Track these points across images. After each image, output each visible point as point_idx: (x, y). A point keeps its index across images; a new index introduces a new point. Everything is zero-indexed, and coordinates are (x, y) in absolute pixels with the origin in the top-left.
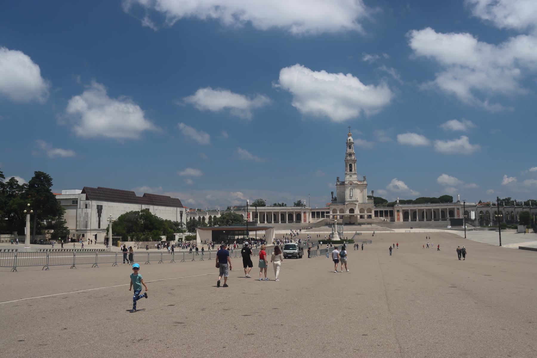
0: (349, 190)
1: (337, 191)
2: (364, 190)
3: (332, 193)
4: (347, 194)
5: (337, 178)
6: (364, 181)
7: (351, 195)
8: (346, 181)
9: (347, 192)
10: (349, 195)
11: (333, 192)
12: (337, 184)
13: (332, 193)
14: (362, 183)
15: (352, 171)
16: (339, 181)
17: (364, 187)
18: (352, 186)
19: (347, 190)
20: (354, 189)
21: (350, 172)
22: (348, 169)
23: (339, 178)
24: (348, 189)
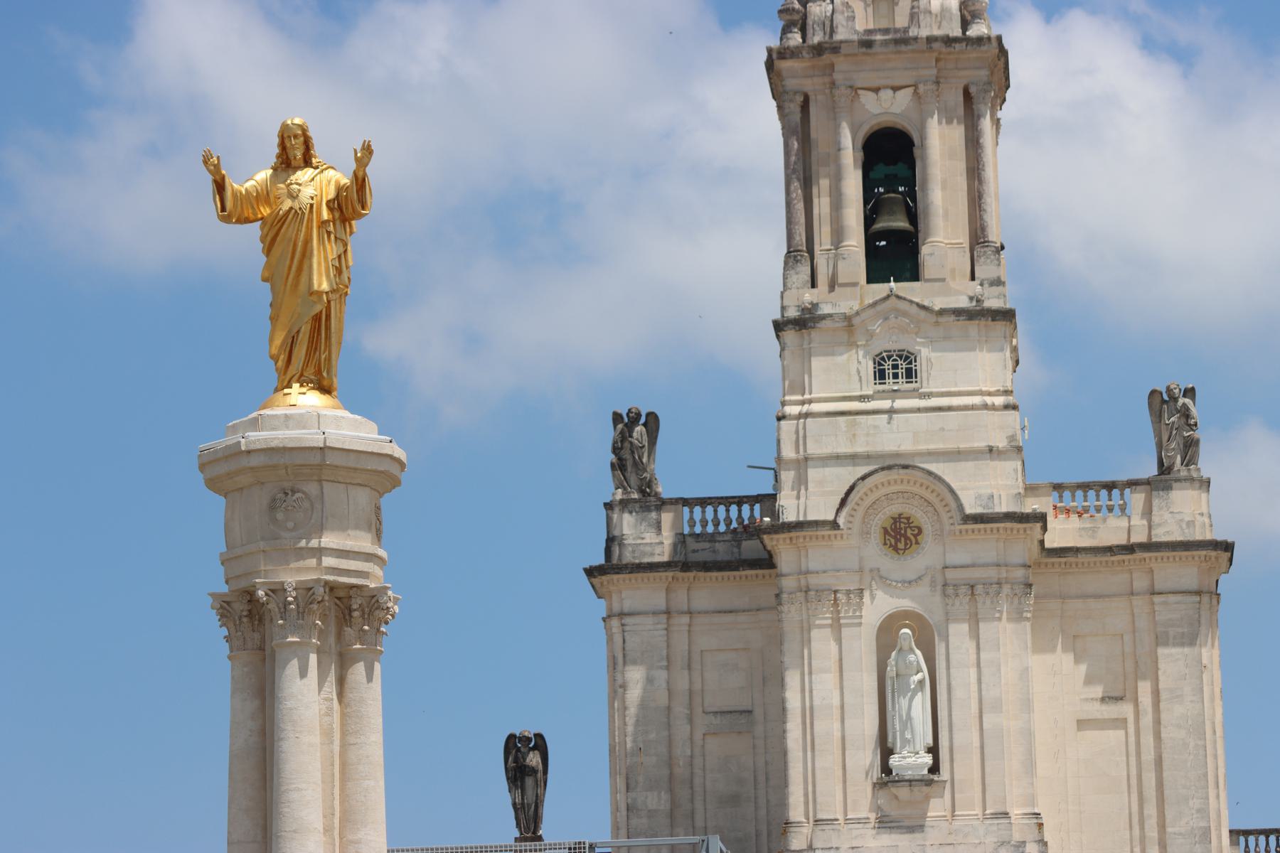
0: (862, 644)
1: (617, 689)
2: (1172, 660)
4: (827, 727)
5: (625, 422)
6: (1164, 478)
7: (911, 760)
8: (803, 463)
9: (825, 687)
10: (865, 757)
11: (540, 744)
12: (612, 541)
14: (1112, 531)
15: (913, 273)
16: (646, 488)
17: (1172, 610)
18: (927, 556)
19: (822, 644)
20: (959, 632)
21: (880, 289)
22: (838, 235)
23: (652, 422)
24: (837, 627)
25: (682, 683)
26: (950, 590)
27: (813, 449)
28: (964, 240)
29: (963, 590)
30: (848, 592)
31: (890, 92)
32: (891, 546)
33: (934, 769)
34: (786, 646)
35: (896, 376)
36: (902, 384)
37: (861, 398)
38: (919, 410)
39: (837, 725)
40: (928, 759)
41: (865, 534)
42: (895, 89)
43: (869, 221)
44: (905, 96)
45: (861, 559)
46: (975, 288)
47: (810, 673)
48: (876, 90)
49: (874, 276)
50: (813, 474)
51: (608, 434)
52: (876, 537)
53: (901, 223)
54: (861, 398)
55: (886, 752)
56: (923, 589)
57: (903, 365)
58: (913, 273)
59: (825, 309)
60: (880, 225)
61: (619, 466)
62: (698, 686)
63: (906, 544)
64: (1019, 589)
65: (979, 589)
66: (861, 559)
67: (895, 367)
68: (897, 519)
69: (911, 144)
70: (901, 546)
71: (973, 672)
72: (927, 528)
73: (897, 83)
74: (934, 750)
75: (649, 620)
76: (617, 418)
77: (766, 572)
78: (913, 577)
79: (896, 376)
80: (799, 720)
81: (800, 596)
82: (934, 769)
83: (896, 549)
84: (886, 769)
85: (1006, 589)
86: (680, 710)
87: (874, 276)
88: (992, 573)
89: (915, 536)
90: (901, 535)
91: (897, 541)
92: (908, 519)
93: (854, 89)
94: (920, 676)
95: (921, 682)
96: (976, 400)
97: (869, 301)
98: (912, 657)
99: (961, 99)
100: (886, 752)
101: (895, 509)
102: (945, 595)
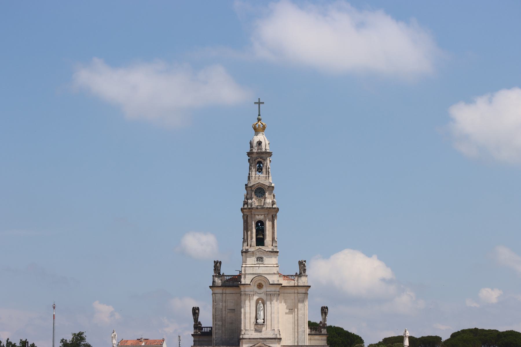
0: (253, 303)
2: (300, 305)
3: (195, 312)
4: (248, 315)
6: (299, 275)
8: (245, 274)
9: (248, 309)
11: (198, 309)
12: (214, 282)
13: (195, 312)
14: (292, 283)
15: (263, 245)
16: (219, 273)
17: (301, 296)
18: (264, 290)
19: (247, 302)
20: (268, 303)
21: (258, 247)
22: (252, 238)
23: (220, 263)
24: (250, 300)
25: (224, 305)
26: (267, 295)
27: (247, 272)
28: (271, 239)
29: (269, 295)
30: (252, 295)
34: (242, 303)
36: (261, 262)
37: (255, 264)
38: (263, 267)
39: (249, 315)
41: (254, 286)
42: (261, 215)
43: (257, 235)
44: (263, 216)
46: (272, 247)
47: (245, 307)
48: (258, 215)
49: (257, 245)
50: (247, 276)
51: (213, 264)
53: (262, 237)
54: (255, 264)
56: (263, 295)
58: (263, 245)
59: (249, 250)
60: (258, 237)
61: (215, 270)
62: (226, 305)
64: (278, 295)
65: (272, 295)
66: (254, 289)
68: (259, 283)
69: (263, 223)
70: (260, 288)
71: (270, 307)
72: (264, 285)
73: (262, 214)
75: (219, 295)
76: (215, 262)
77: (238, 288)
79: (260, 261)
80: (243, 314)
81: (244, 295)
83: (259, 288)
86: (224, 309)
87: (257, 245)
88: (274, 293)
93: (255, 215)
94: (262, 308)
95: (262, 309)
96: (272, 265)
97: (256, 249)
98: (261, 305)
99: (271, 217)
101: (259, 282)
102: (266, 296)
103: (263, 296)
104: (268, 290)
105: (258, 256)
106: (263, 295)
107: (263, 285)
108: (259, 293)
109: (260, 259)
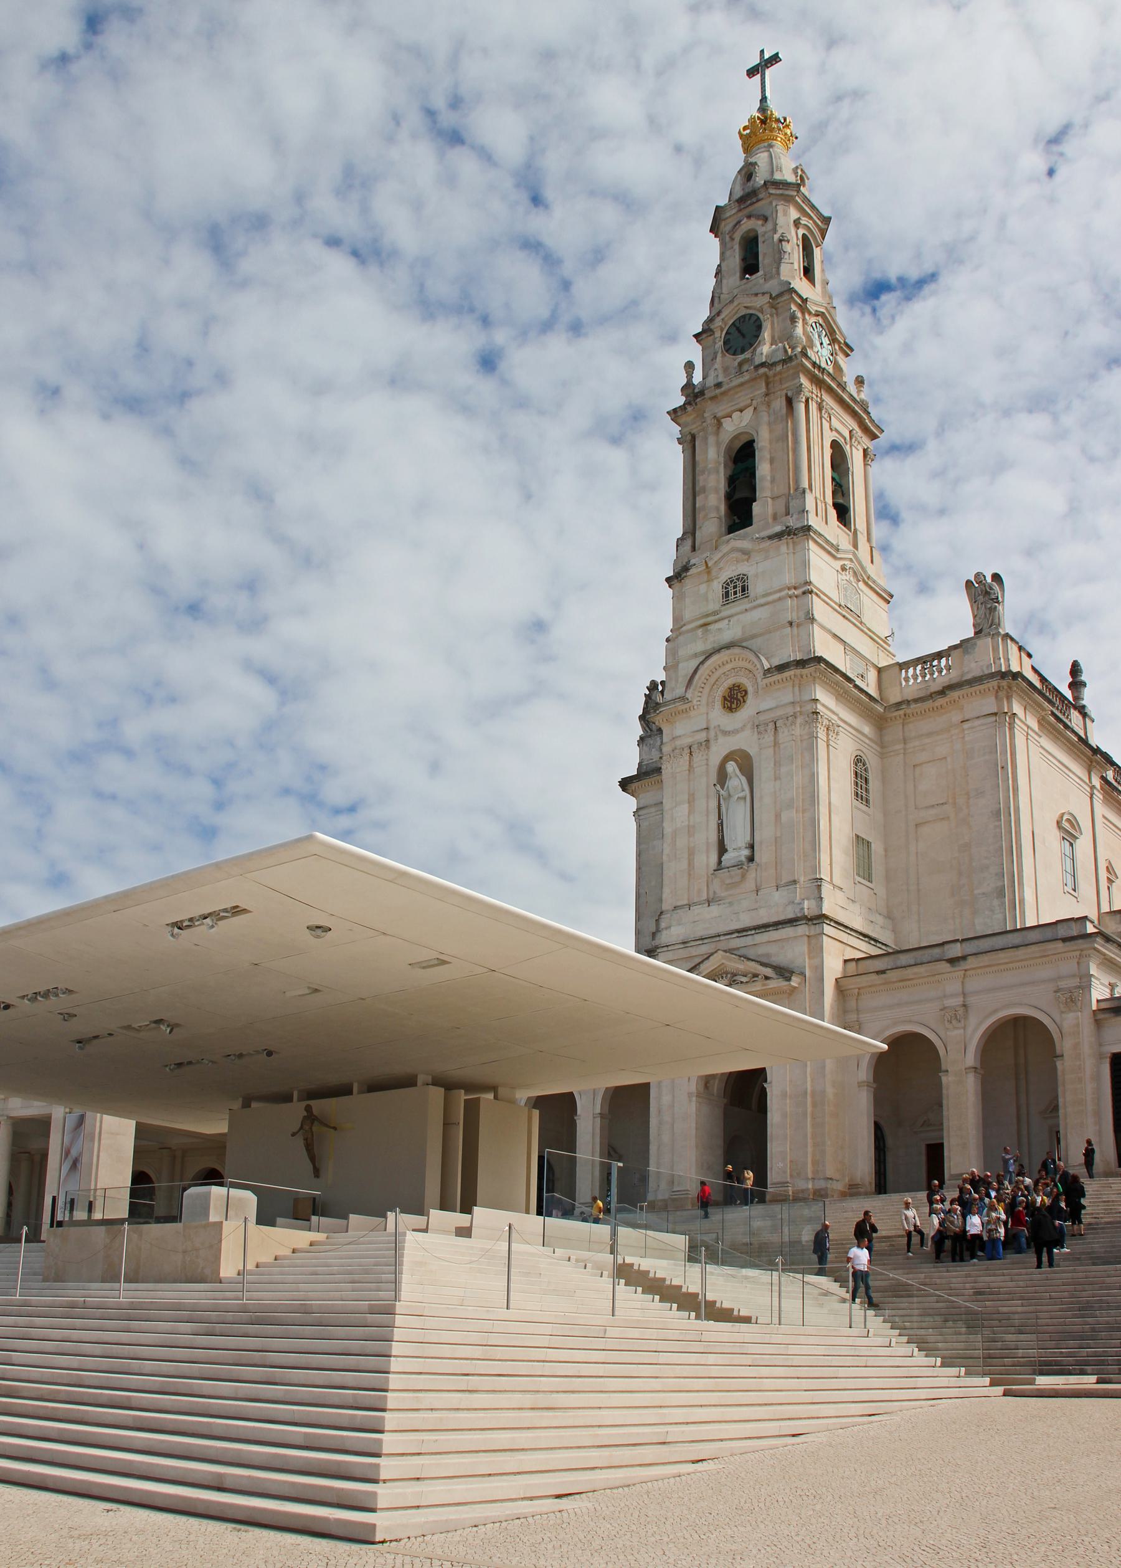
0: (705, 778)
26: (762, 728)
31: (739, 413)
32: (728, 707)
33: (751, 859)
35: (735, 593)
40: (747, 852)
41: (710, 704)
44: (749, 413)
45: (708, 721)
52: (718, 704)
55: (722, 849)
56: (747, 733)
57: (739, 584)
63: (737, 704)
66: (708, 721)
67: (735, 587)
70: (734, 706)
72: (750, 690)
73: (742, 405)
74: (752, 847)
78: (738, 725)
82: (751, 859)
84: (720, 862)
85: (799, 721)
88: (790, 710)
89: (743, 697)
90: (733, 698)
91: (732, 703)
92: (739, 686)
95: (745, 798)
100: (722, 849)
101: (730, 682)
102: (759, 733)
103: (745, 741)
104: (764, 706)
105: (725, 576)
106: (747, 733)
107: (746, 692)
108: (727, 729)
109: (735, 587)
